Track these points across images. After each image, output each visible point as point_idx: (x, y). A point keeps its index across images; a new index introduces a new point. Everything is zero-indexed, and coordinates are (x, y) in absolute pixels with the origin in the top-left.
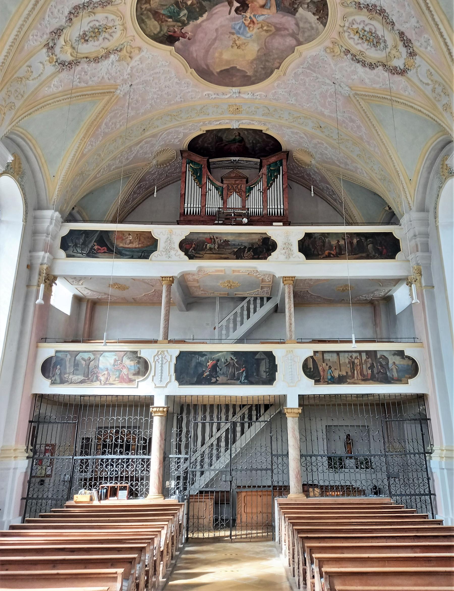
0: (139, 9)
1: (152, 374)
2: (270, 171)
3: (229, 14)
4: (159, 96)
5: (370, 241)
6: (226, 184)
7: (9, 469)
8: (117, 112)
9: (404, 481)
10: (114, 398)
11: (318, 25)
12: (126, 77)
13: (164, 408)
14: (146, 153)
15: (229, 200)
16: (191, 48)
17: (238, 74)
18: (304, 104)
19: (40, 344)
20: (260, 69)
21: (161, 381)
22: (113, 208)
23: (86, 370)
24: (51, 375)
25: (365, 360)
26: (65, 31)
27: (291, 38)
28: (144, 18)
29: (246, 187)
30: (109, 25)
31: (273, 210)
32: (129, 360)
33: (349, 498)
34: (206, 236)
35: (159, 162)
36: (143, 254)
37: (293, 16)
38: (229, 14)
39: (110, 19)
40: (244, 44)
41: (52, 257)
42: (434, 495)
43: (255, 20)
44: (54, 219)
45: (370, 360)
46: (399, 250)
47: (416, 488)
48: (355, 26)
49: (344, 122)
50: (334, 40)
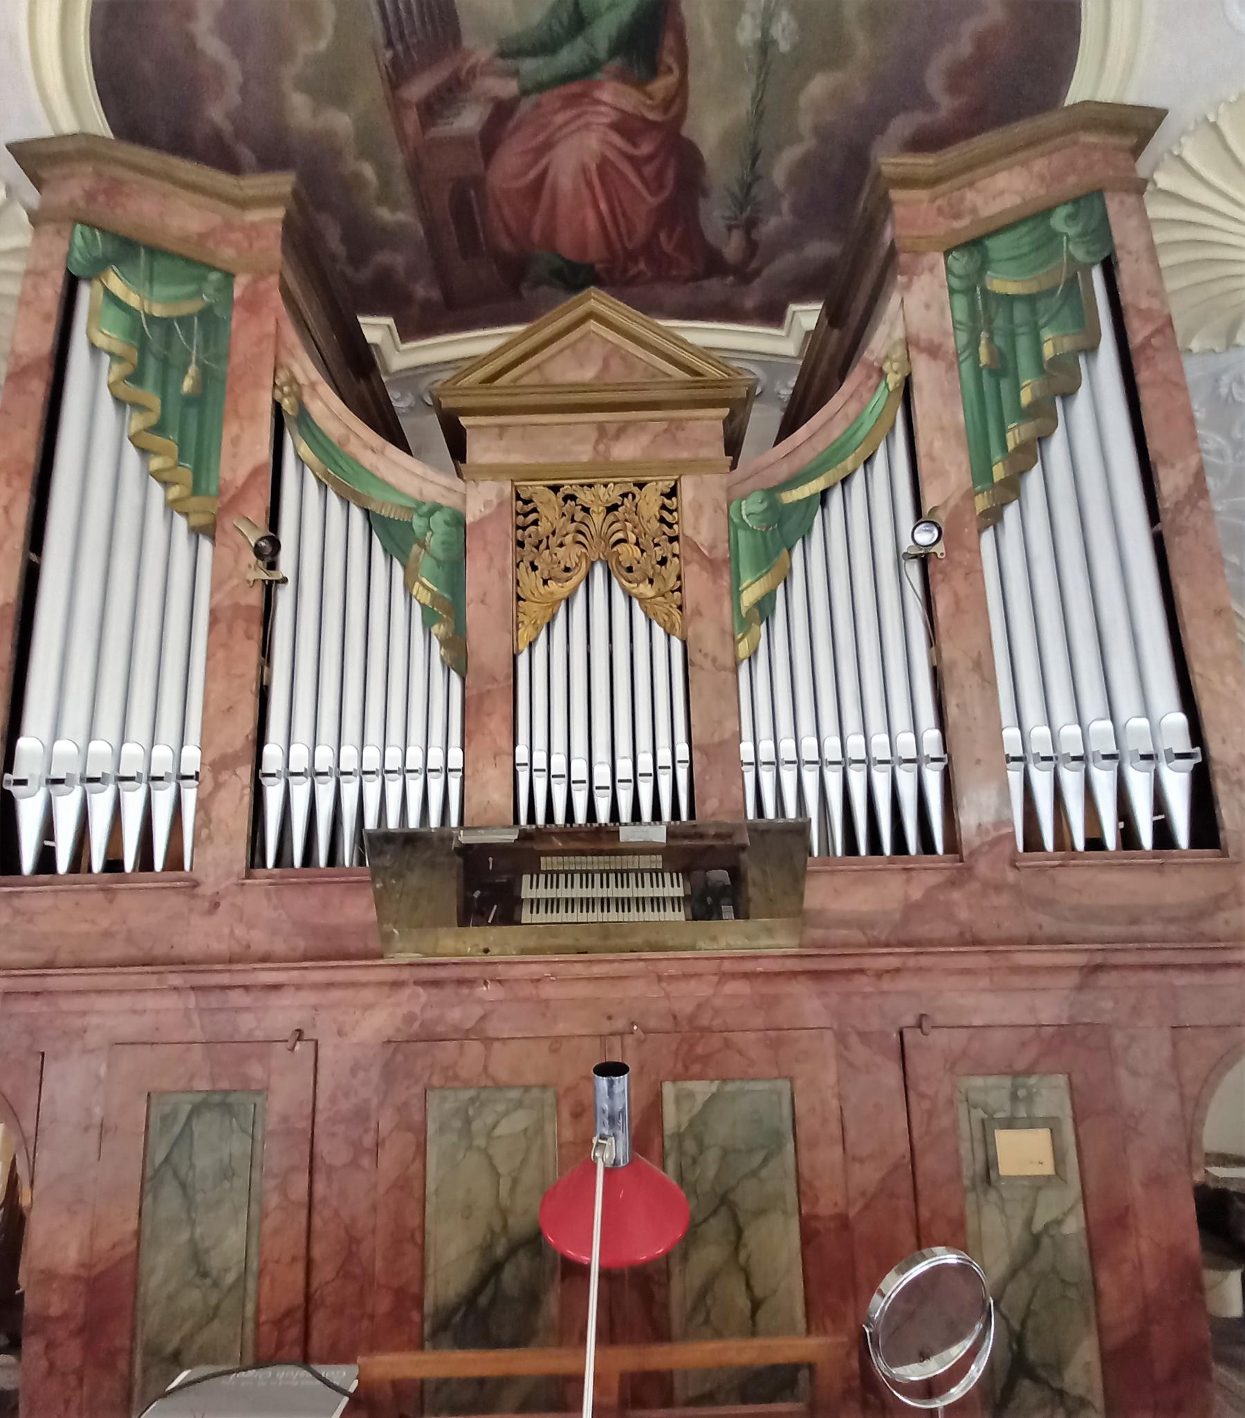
6: (494, 472)
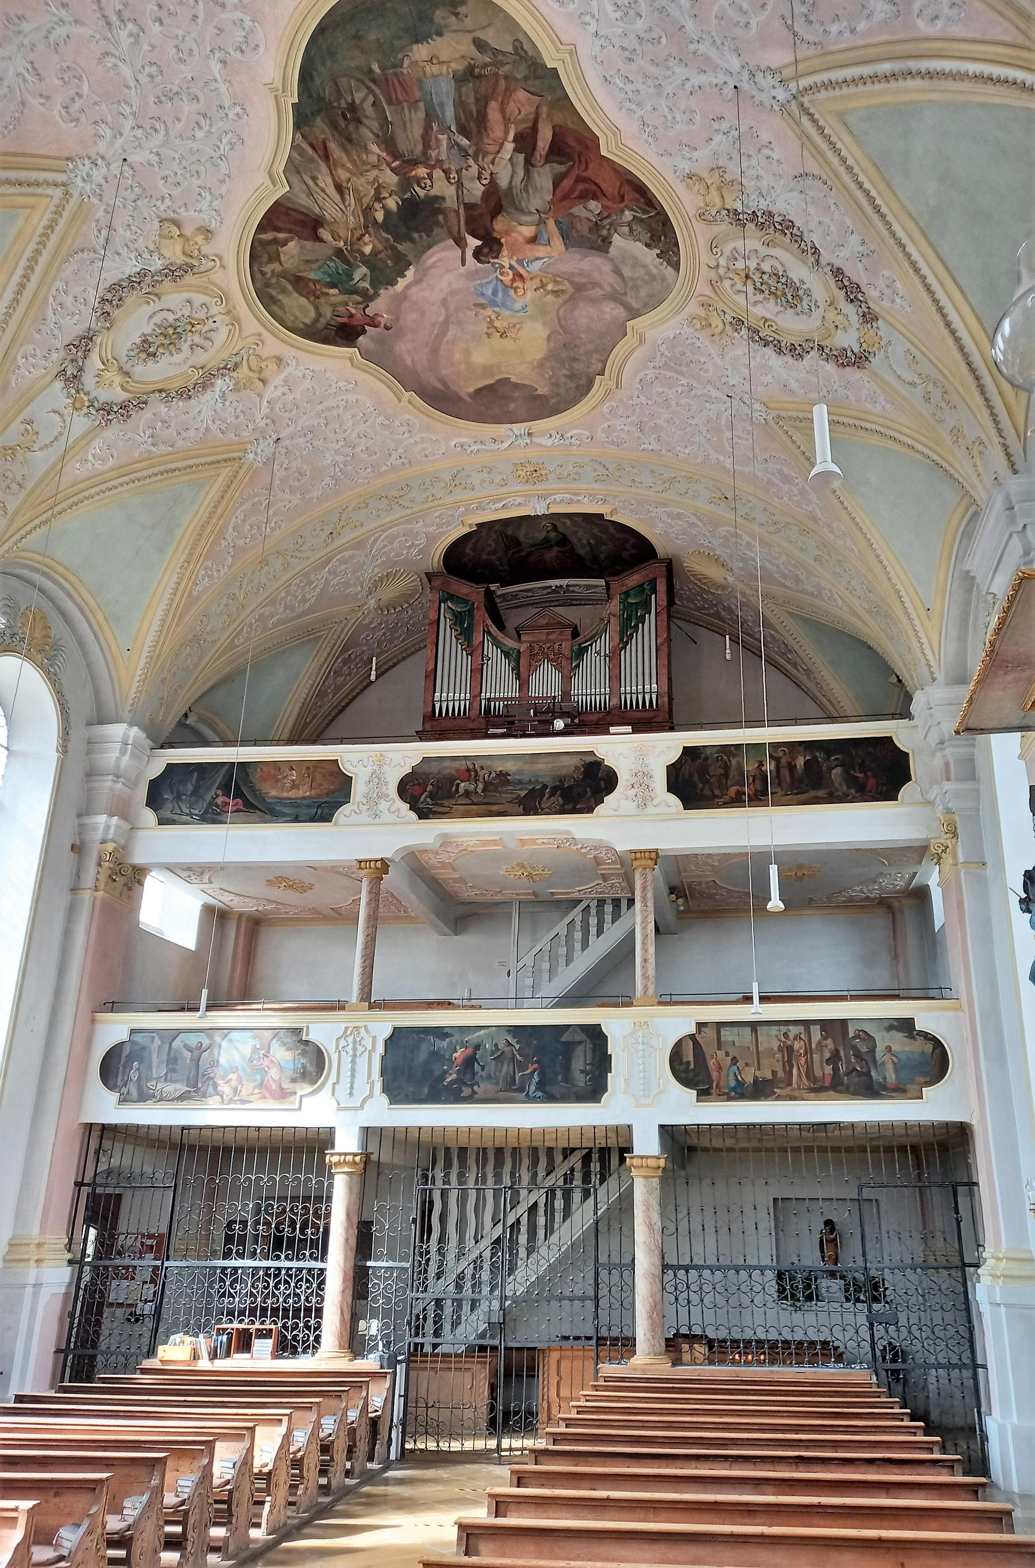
0: (258, 276)
1: (333, 1078)
2: (626, 606)
3: (463, 263)
4: (348, 458)
5: (836, 759)
7: (23, 1286)
8: (256, 500)
9: (910, 1332)
10: (254, 1134)
11: (662, 268)
12: (262, 424)
13: (355, 1155)
14: (347, 585)
15: (533, 679)
16: (397, 348)
17: (517, 394)
18: (678, 448)
19: (100, 1016)
20: (563, 380)
21: (351, 1094)
22: (289, 711)
23: (193, 1072)
24: (119, 1083)
25: (819, 1043)
26: (98, 340)
27: (612, 305)
28: (274, 293)
29: (572, 646)
30: (196, 316)
31: (634, 697)
32: (284, 1048)
33: (775, 1368)
34: (457, 764)
35: (382, 603)
36: (319, 812)
37: (603, 254)
38: (463, 263)
39: (196, 304)
40: (514, 326)
41: (125, 825)
42: (984, 1367)
43: (522, 271)
44: (130, 742)
45: (829, 1041)
46: (909, 779)
47: (938, 1349)
48: (740, 265)
49: (769, 482)
50: (702, 298)
